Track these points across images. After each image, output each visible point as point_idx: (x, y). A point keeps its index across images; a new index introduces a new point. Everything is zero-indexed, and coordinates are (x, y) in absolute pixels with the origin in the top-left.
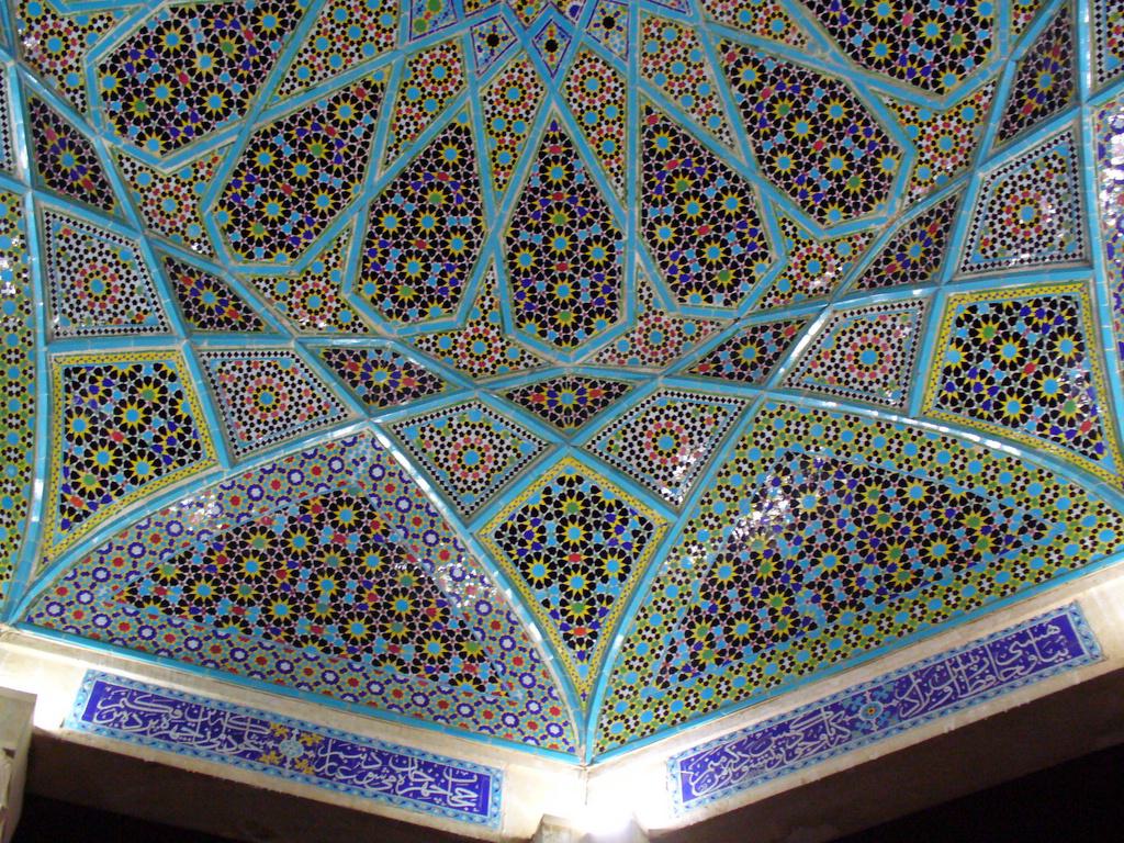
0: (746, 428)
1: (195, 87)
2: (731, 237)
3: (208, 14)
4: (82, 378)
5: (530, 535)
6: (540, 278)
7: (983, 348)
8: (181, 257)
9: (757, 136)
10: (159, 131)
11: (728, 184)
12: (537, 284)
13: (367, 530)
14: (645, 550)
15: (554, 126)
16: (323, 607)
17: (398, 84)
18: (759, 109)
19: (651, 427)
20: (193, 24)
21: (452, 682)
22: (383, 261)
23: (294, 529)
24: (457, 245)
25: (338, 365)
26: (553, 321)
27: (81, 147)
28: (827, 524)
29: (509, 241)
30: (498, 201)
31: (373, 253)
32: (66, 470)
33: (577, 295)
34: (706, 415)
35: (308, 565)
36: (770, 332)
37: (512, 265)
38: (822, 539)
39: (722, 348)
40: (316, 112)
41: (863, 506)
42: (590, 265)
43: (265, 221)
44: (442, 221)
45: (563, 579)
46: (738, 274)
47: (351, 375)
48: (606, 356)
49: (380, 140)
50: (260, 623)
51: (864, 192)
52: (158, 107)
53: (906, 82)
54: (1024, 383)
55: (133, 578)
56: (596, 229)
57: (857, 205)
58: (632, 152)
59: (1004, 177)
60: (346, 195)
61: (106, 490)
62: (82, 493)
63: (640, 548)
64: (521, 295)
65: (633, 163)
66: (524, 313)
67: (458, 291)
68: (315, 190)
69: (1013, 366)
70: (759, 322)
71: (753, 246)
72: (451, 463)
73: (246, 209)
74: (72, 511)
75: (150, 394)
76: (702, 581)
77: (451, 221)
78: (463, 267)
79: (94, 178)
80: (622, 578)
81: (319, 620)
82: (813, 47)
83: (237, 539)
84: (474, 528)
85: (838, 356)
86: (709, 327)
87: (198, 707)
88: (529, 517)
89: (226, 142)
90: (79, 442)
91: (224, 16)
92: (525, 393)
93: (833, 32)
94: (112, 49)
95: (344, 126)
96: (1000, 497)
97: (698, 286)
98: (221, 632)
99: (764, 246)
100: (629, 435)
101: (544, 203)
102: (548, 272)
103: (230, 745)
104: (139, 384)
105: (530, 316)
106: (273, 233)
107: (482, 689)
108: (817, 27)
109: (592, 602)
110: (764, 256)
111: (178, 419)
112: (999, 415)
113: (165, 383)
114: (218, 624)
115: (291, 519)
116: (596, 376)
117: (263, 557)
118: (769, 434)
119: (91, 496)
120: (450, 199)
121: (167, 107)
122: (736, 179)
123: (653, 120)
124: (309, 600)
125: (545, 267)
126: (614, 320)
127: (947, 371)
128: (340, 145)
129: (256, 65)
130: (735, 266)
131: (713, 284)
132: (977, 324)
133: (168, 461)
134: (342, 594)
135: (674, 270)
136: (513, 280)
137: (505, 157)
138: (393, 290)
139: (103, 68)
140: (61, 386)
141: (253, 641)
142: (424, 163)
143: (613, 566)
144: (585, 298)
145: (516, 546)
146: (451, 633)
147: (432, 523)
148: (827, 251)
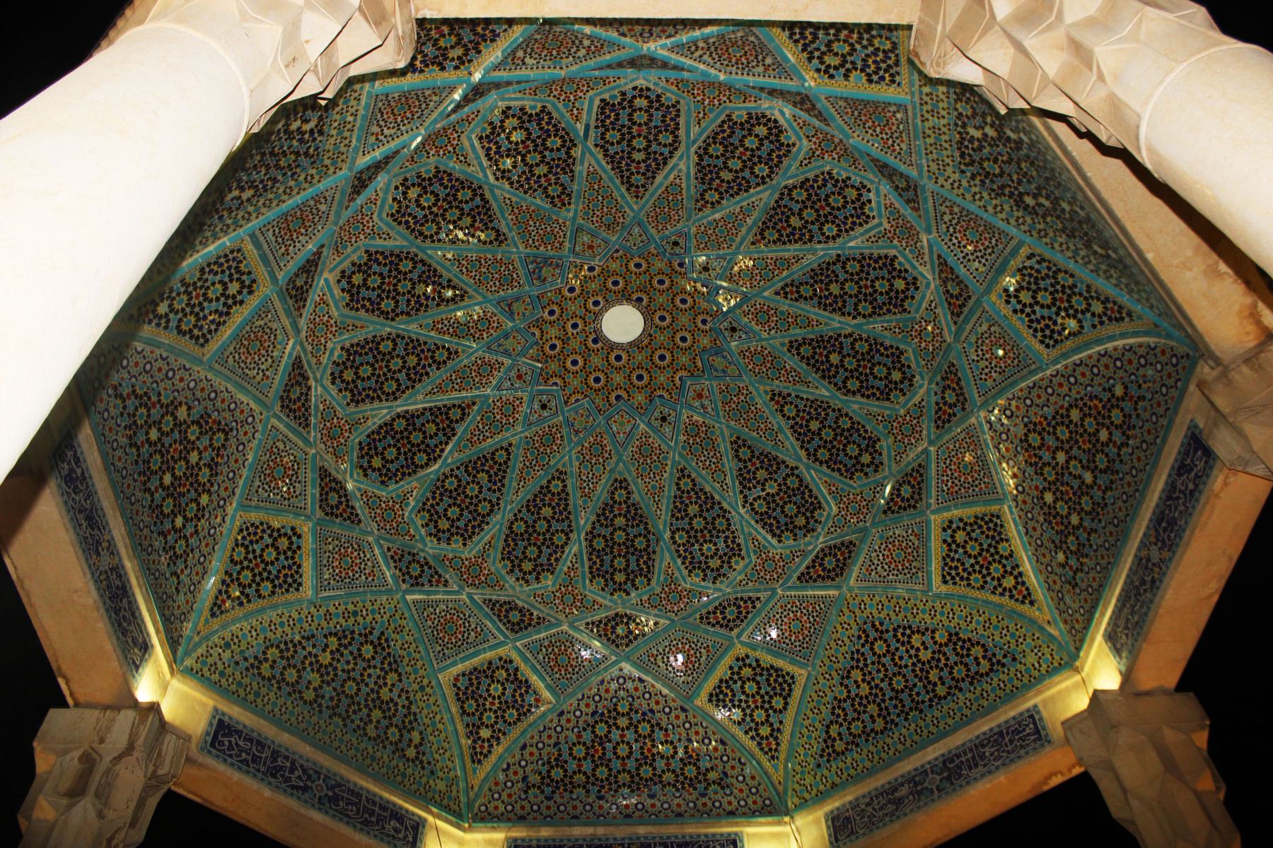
3: (744, 487)
4: (949, 574)
6: (875, 299)
10: (812, 512)
11: (786, 198)
15: (777, 293)
21: (1138, 415)
22: (878, 389)
23: (1042, 474)
25: (944, 422)
26: (903, 292)
27: (823, 554)
29: (854, 318)
31: (874, 395)
35: (1063, 475)
37: (870, 316)
38: (1014, 167)
40: (792, 427)
42: (862, 271)
46: (847, 186)
47: (950, 415)
50: (1093, 520)
52: (799, 512)
53: (682, 121)
57: (776, 127)
60: (839, 410)
61: (1015, 573)
71: (824, 180)
73: (854, 466)
74: (1024, 597)
75: (960, 536)
80: (1072, 276)
81: (1094, 482)
82: (680, 171)
89: (817, 478)
91: (744, 479)
92: (952, 313)
93: (665, 164)
94: (769, 537)
97: (861, 208)
101: (826, 298)
102: (871, 295)
103: (1145, 591)
105: (902, 306)
108: (666, 172)
109: (1092, 298)
111: (976, 523)
113: (954, 526)
114: (1091, 546)
118: (950, 181)
119: (1017, 583)
122: (782, 194)
128: (809, 413)
131: (858, 200)
138: (896, 383)
139: (780, 541)
141: (1100, 530)
144: (885, 272)
145: (1056, 336)
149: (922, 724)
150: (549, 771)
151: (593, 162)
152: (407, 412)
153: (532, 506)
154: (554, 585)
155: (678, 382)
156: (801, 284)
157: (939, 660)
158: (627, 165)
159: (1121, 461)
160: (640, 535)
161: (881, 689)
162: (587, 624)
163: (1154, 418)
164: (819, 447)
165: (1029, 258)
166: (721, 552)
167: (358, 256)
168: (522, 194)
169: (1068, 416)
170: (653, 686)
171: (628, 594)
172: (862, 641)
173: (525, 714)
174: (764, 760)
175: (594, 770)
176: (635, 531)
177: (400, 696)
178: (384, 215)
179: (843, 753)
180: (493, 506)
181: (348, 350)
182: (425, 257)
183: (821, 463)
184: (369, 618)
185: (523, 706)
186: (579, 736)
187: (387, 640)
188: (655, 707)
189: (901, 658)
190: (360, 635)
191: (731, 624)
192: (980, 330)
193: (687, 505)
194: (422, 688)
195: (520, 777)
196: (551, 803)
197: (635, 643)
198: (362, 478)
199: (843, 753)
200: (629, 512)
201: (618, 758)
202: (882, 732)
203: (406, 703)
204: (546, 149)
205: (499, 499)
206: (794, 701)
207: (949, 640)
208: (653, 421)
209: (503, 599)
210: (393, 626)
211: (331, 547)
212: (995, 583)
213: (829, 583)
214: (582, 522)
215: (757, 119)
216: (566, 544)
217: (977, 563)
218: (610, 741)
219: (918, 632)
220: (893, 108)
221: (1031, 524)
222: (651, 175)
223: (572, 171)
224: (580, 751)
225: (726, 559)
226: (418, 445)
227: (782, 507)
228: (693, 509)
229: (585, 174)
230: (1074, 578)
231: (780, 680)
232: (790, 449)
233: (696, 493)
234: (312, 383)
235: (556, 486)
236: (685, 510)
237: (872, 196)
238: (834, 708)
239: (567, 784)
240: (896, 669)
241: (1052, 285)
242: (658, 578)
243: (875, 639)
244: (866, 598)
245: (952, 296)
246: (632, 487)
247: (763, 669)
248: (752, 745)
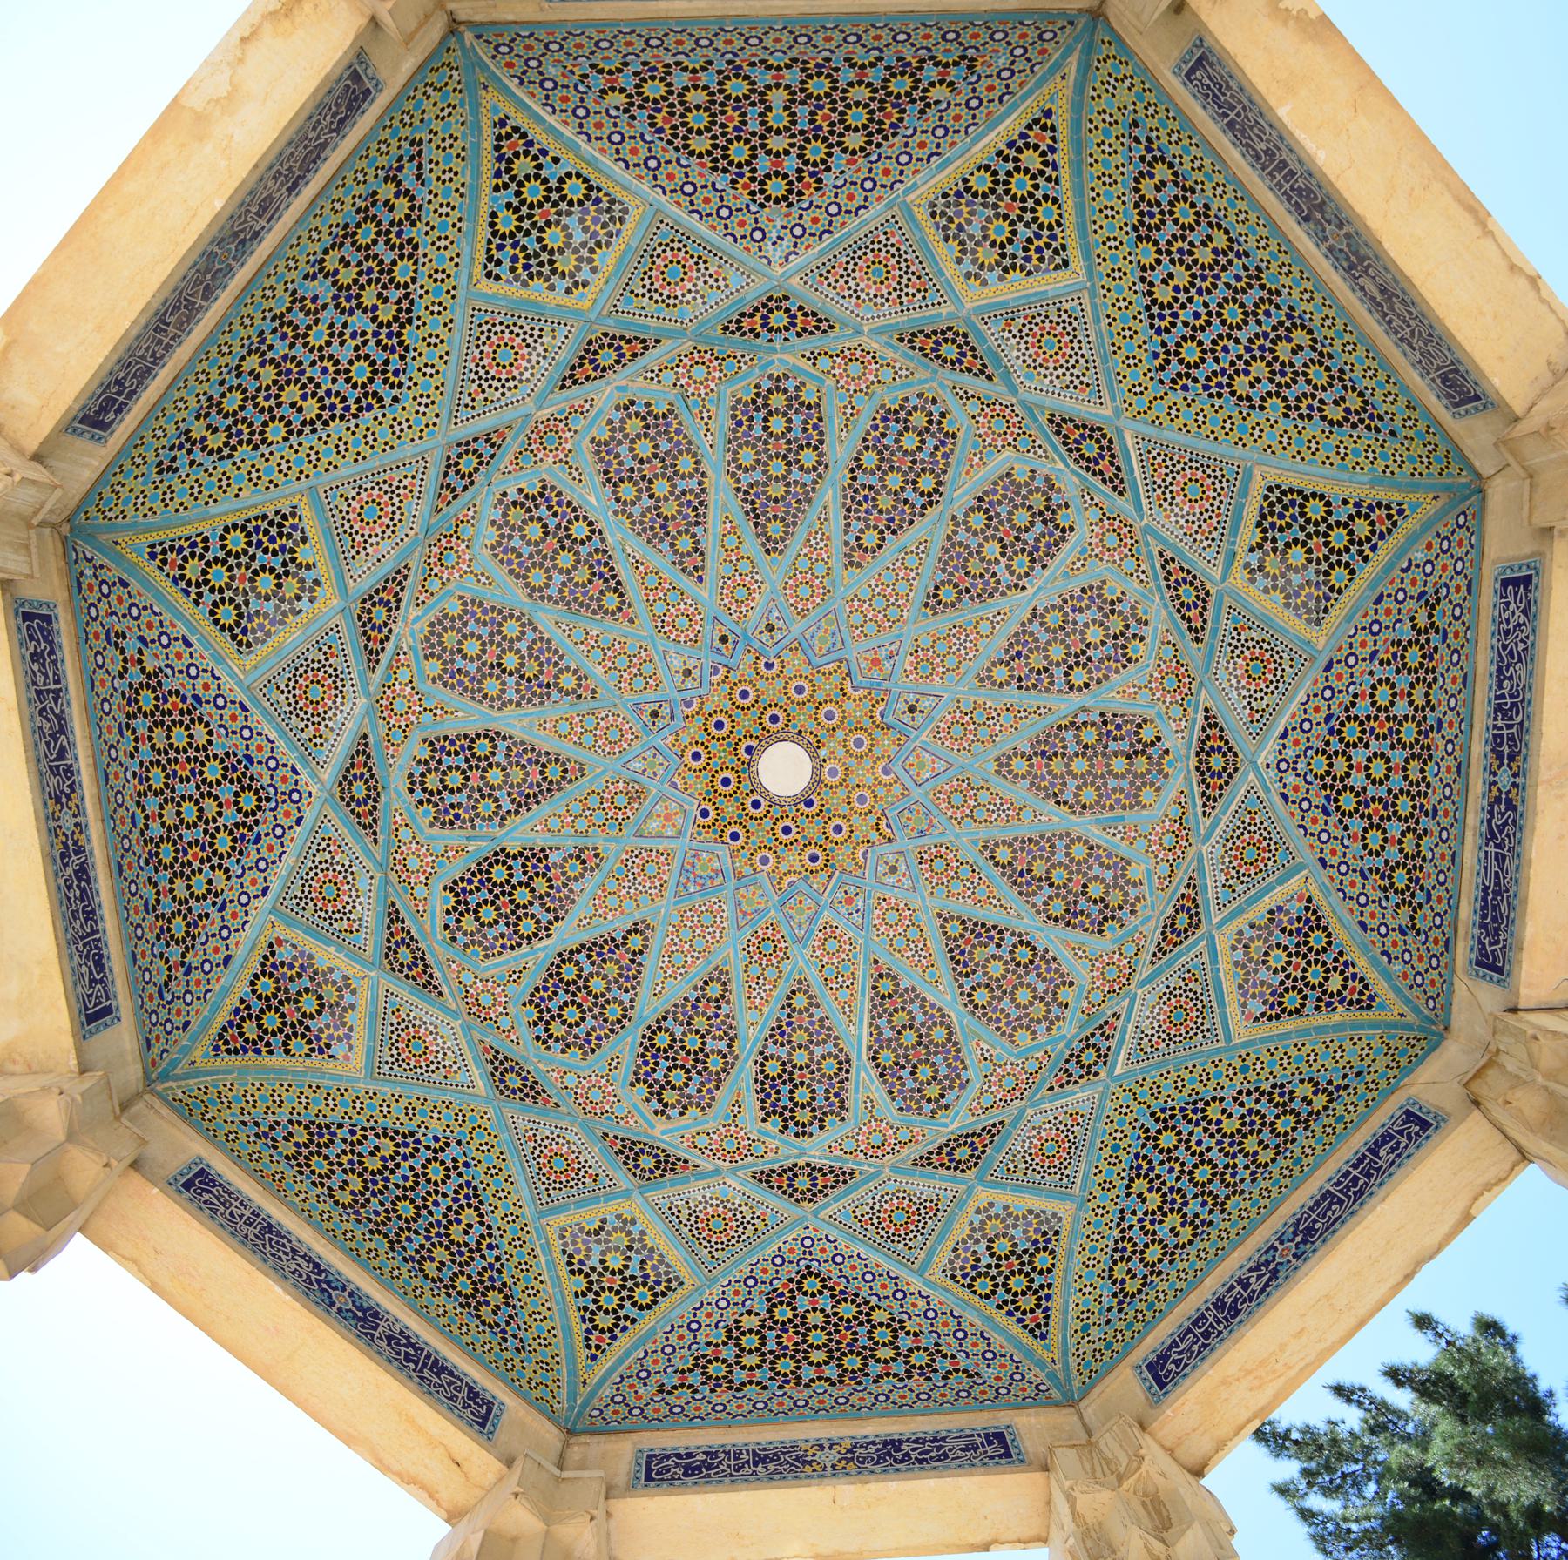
0: (444, 404)
17: (834, 573)
24: (747, 457)
29: (703, 475)
30: (725, 505)
33: (632, 449)
44: (765, 472)
46: (507, 523)
56: (636, 511)
64: (678, 432)
69: (255, 573)
77: (757, 475)
97: (534, 498)
100: (540, 349)
110: (493, 548)
126: (593, 441)
130: (512, 528)
137: (731, 541)
138: (789, 399)
146: (641, 107)
156: (676, 552)
157: (1180, 251)
161: (1250, 341)
165: (498, 278)
172: (1189, 383)
174: (1405, 527)
183: (939, 483)
192: (652, 308)
219: (1151, 293)
231: (1278, 509)
238: (1301, 416)
240: (1216, 321)
243: (1181, 361)
244: (1125, 386)
247: (1265, 539)
248: (1386, 550)
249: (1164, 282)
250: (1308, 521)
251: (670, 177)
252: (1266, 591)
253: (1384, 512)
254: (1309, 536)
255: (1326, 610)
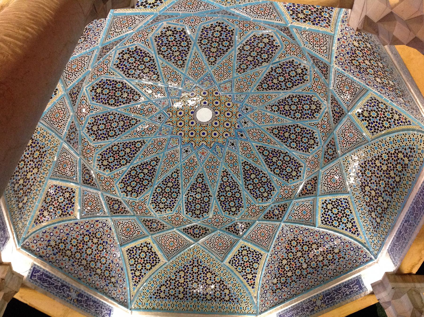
1: (201, 201)
2: (304, 135)
3: (191, 190)
4: (232, 261)
5: (328, 218)
7: (368, 117)
8: (227, 226)
9: (288, 116)
10: (204, 212)
11: (294, 127)
12: (283, 173)
13: (300, 243)
14: (350, 204)
15: (257, 146)
16: (305, 266)
18: (283, 111)
19: (328, 180)
20: (191, 193)
25: (268, 217)
26: (293, 176)
28: (375, 176)
29: (271, 171)
31: (254, 194)
32: (244, 278)
34: (335, 170)
35: (296, 259)
36: (330, 145)
37: (276, 174)
39: (325, 155)
40: (221, 184)
41: (378, 167)
43: (233, 207)
45: (341, 221)
46: (313, 139)
47: (271, 217)
48: (308, 173)
49: (235, 177)
50: (297, 278)
51: (317, 107)
52: (200, 209)
53: (300, 85)
54: (383, 118)
55: (271, 288)
56: (282, 155)
58: (274, 138)
59: (335, 85)
60: (240, 190)
61: (254, 275)
62: (251, 279)
63: (349, 204)
64: (283, 177)
65: (275, 139)
66: (287, 179)
67: (273, 186)
68: (234, 195)
70: (326, 144)
71: (310, 133)
72: (302, 217)
73: (228, 208)
74: (252, 284)
75: (245, 253)
76: (365, 204)
78: (269, 182)
79: (203, 229)
80: (351, 213)
81: (306, 269)
83: (281, 264)
84: (317, 226)
85: (346, 140)
86: (319, 152)
87: (298, 307)
88: (324, 215)
89: (214, 203)
90: (242, 271)
91: (193, 187)
93: (278, 90)
94: (185, 210)
95: (227, 181)
96: (401, 146)
97: (309, 148)
98: (292, 286)
99: (312, 131)
101: (269, 159)
102: (283, 169)
104: (241, 253)
105: (288, 179)
106: (236, 207)
107: (345, 258)
108: (275, 91)
109: (350, 222)
110: (314, 132)
111: (253, 252)
112: (385, 127)
114: (290, 285)
115: (286, 252)
116: (310, 178)
117: (287, 264)
119: (252, 278)
120: (255, 174)
121: (201, 208)
122: (294, 125)
123: (270, 130)
124: (301, 266)
125: (282, 170)
126: (302, 166)
127: (367, 127)
128: (230, 184)
129: (205, 188)
131: (311, 145)
132: (362, 114)
133: (258, 260)
134: (305, 260)
135: (302, 149)
136: (279, 176)
138: (263, 196)
139: (187, 214)
140: (231, 266)
142: (245, 173)
143: (347, 212)
145: (327, 222)
147: (309, 231)
148: (323, 122)
149: (197, 305)
150: (59, 243)
151: (263, 71)
152: (125, 84)
153: (125, 145)
154: (107, 176)
155: (200, 144)
158: (269, 80)
159: (322, 269)
160: (148, 180)
162: (107, 197)
163: (345, 266)
164: (223, 196)
166: (166, 204)
167: (179, 28)
168: (236, 59)
169: (311, 245)
170: (113, 234)
171: (127, 196)
172: (191, 264)
173: (64, 215)
175: (75, 253)
176: (147, 178)
177: (32, 179)
178: (203, 25)
179: (163, 298)
180: (115, 135)
181: (137, 49)
182: (191, 48)
184: (46, 142)
185: (65, 212)
186: (77, 236)
187: (45, 155)
188: (109, 242)
189: (200, 278)
190: (39, 146)
191: (152, 229)
193: (169, 182)
194: (40, 182)
195: (48, 239)
196: (54, 257)
197: (117, 214)
198: (89, 91)
199: (163, 298)
200: (151, 170)
201: (86, 253)
202: (181, 299)
203: (32, 184)
204: (260, 55)
205: (119, 134)
206: (154, 269)
207: (220, 282)
208: (183, 149)
209: (88, 168)
210: (51, 151)
211: (59, 106)
212: (245, 274)
213: (193, 237)
214: (135, 162)
215: (318, 104)
216: (124, 165)
217: (244, 264)
218: (87, 245)
219: (211, 273)
220: (361, 138)
221: (271, 265)
222: (269, 88)
223: (256, 67)
224: (74, 242)
225: (166, 207)
226: (116, 97)
227: (196, 204)
228: (170, 184)
229: (256, 71)
230: (276, 290)
231: (154, 259)
232: (214, 190)
233: (175, 180)
234: (114, 48)
235: (138, 145)
236: (167, 183)
237: (316, 147)
238: (167, 280)
239: (63, 252)
241: (342, 210)
242: (141, 197)
243: (196, 266)
245: (306, 189)
246: (159, 164)
247: (151, 251)
249: (210, 277)
250: (147, 263)
251: (317, 235)
252: (142, 244)
253: (137, 281)
254: (144, 261)
255: (128, 254)
